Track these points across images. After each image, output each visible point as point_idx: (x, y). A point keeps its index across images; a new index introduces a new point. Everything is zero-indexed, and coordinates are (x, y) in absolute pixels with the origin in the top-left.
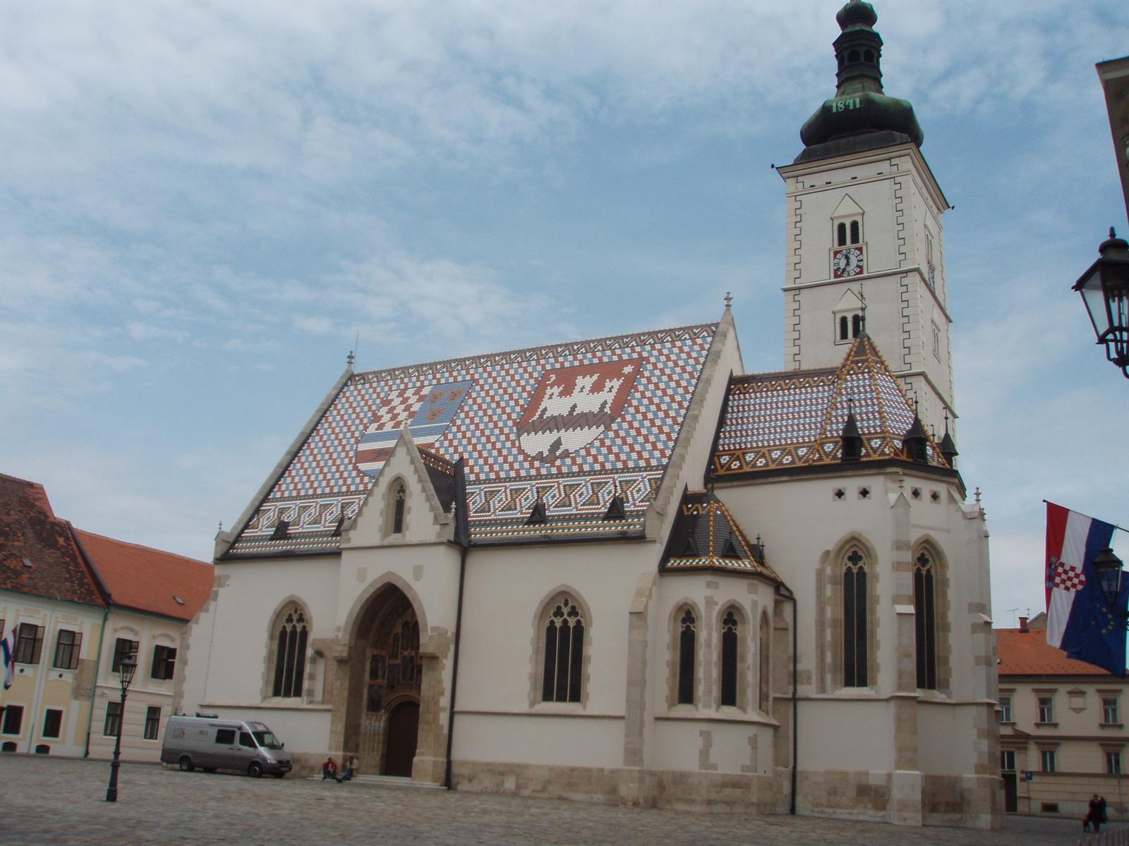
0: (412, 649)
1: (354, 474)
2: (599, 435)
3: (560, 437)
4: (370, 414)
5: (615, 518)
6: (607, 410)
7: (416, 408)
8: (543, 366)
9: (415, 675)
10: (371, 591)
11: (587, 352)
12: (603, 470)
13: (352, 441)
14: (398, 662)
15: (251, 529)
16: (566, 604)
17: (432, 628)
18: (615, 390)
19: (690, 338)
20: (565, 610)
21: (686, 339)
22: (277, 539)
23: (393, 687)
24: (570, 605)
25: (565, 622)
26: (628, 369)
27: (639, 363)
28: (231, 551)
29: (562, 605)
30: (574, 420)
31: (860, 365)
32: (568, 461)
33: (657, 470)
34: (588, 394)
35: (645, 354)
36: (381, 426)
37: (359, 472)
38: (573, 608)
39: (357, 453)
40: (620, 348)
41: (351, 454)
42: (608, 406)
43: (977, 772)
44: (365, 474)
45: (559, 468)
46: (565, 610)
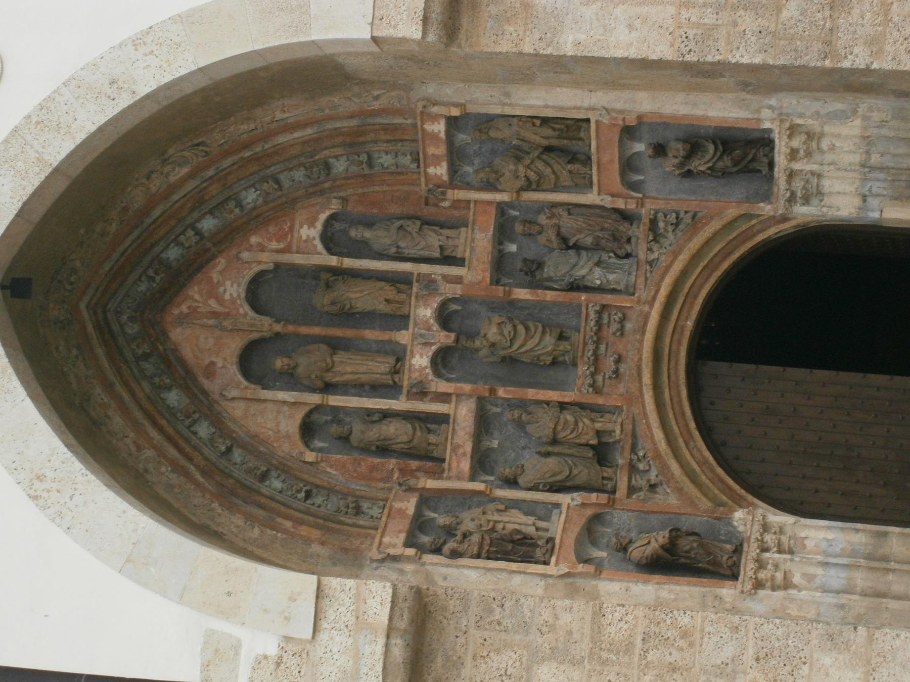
0: (401, 320)
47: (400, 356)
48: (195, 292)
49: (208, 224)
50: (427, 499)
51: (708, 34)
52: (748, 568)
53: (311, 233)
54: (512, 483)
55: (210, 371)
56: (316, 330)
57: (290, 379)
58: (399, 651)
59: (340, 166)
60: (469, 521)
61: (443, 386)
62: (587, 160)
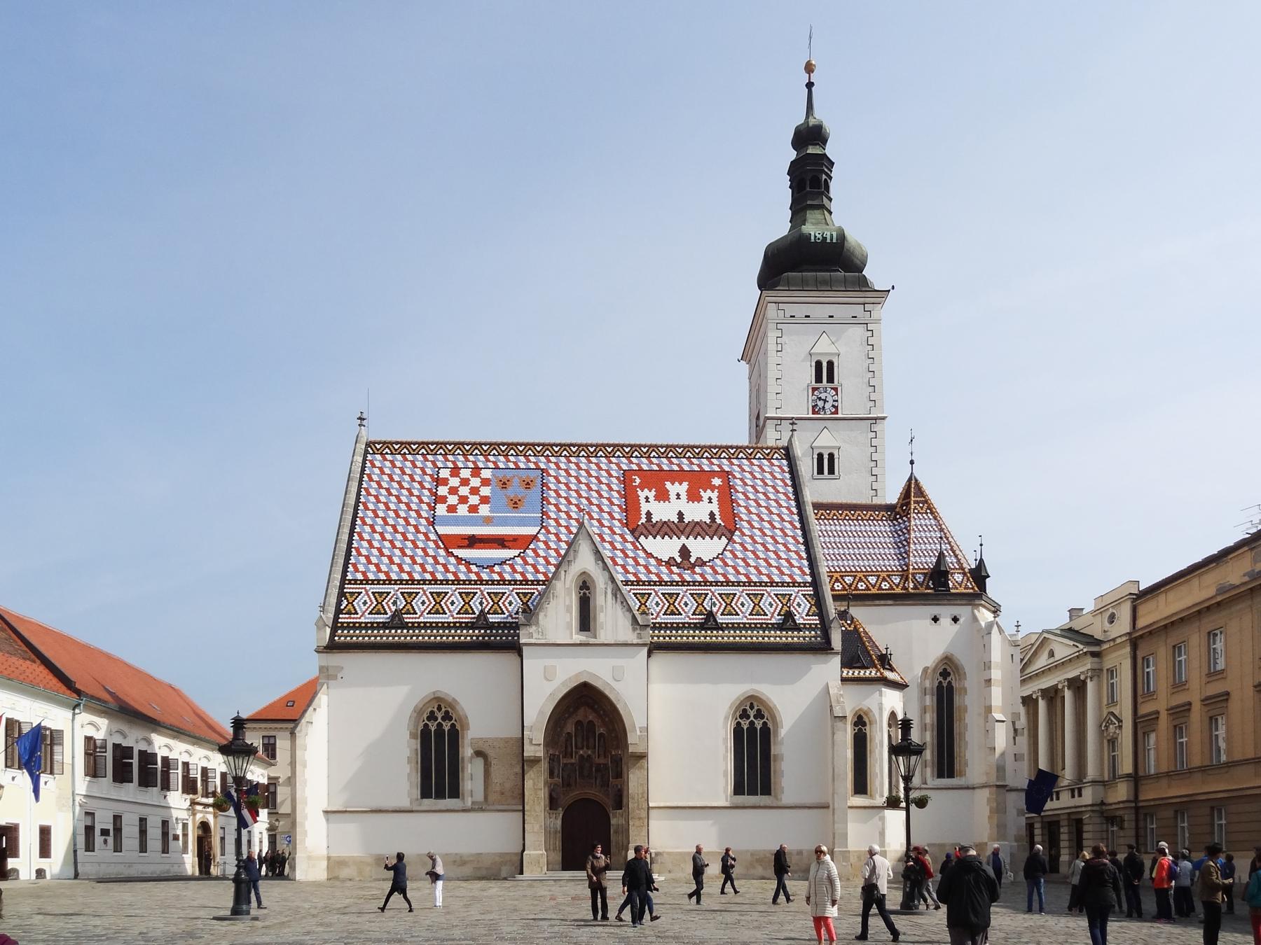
0: (588, 748)
1: (452, 560)
2: (726, 547)
3: (684, 544)
4: (426, 492)
5: (787, 630)
6: (719, 521)
7: (485, 491)
8: (618, 465)
9: (594, 774)
10: (565, 691)
11: (659, 457)
12: (750, 583)
13: (423, 521)
14: (573, 761)
15: (345, 614)
16: (752, 707)
17: (640, 728)
18: (715, 500)
19: (765, 458)
20: (752, 713)
21: (760, 458)
22: (396, 628)
23: (569, 785)
24: (756, 708)
25: (752, 723)
26: (717, 482)
27: (725, 475)
28: (336, 638)
29: (748, 708)
30: (680, 527)
31: (921, 505)
32: (708, 570)
33: (805, 586)
34: (688, 502)
35: (727, 469)
36: (452, 509)
37: (459, 560)
38: (759, 711)
39: (439, 536)
40: (694, 457)
41: (433, 537)
42: (718, 517)
43: (1016, 840)
44: (468, 563)
45: (702, 575)
46: (752, 713)
47: (582, 748)
48: (590, 710)
49: (601, 712)
50: (559, 756)
51: (633, 799)
52: (551, 811)
53: (602, 730)
54: (562, 770)
55: (577, 715)
56: (585, 733)
57: (576, 729)
58: (533, 758)
59: (613, 735)
60: (555, 764)
61: (577, 756)
62: (617, 778)
